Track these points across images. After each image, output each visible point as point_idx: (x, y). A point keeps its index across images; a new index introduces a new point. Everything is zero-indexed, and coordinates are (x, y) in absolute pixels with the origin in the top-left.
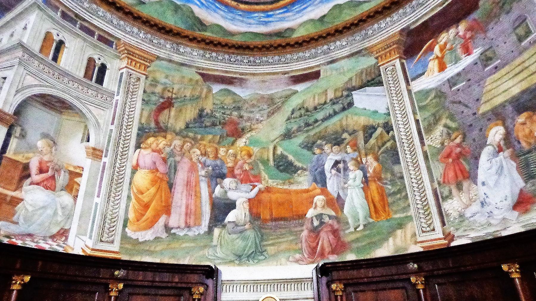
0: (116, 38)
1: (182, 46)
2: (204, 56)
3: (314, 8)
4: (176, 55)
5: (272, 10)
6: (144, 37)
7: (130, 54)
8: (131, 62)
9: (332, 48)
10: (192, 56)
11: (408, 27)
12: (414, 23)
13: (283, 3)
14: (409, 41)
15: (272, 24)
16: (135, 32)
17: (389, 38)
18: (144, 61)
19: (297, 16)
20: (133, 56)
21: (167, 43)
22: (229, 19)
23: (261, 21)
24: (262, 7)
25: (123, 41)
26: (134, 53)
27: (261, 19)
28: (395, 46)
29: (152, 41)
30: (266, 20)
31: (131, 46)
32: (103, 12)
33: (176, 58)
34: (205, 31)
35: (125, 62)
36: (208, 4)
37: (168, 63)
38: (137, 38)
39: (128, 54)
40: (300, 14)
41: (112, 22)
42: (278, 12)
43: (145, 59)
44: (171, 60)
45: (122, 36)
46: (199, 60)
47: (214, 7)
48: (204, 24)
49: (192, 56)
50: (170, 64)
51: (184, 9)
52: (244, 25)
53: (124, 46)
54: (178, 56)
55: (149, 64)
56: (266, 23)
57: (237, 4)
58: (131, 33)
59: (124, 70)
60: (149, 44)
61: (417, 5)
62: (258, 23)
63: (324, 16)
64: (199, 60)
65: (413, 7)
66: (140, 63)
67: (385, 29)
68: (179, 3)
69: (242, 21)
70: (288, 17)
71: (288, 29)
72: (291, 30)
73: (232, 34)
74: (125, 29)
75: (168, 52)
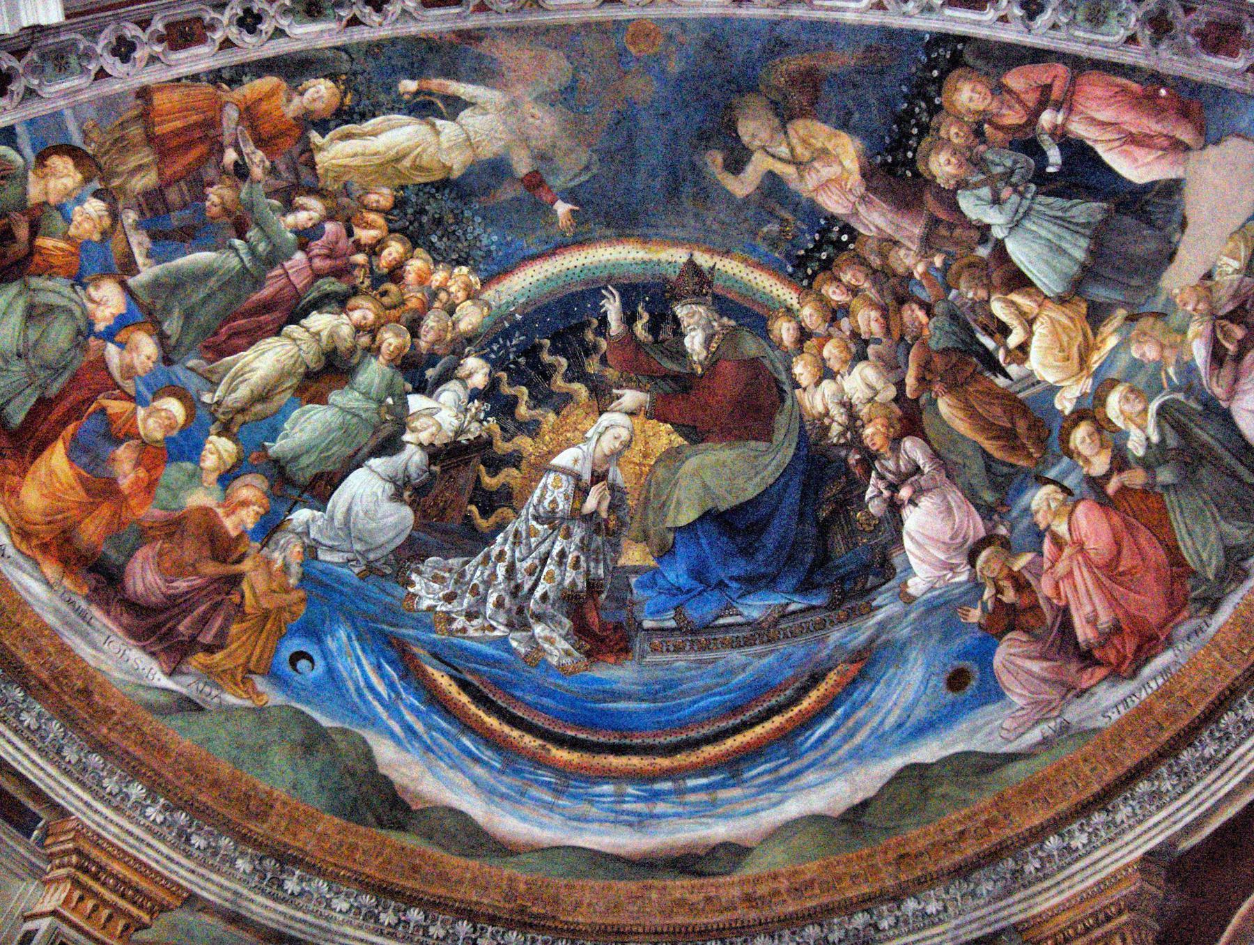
0: (55, 806)
1: (297, 872)
2: (372, 916)
3: (827, 774)
4: (260, 899)
5: (668, 774)
6: (160, 819)
7: (86, 871)
8: (81, 899)
9: (884, 924)
10: (326, 912)
11: (1171, 843)
12: (1189, 830)
13: (713, 753)
14: (1177, 902)
15: (664, 823)
16: (133, 798)
17: (1101, 887)
18: (134, 903)
19: (762, 801)
20: (95, 877)
21: (243, 854)
22: (503, 796)
23: (623, 812)
24: (635, 762)
25: (78, 819)
26: (101, 868)
27: (625, 806)
28: (1125, 918)
29: (188, 840)
30: (641, 807)
31: (97, 841)
32: (40, 716)
33: (262, 908)
34: (401, 827)
35: (56, 895)
36: (434, 741)
37: (222, 925)
38: (130, 818)
39: (79, 867)
40: (775, 796)
41: (59, 751)
42: (691, 783)
43: (137, 896)
44: (238, 914)
45: (80, 805)
46: (348, 930)
47: (456, 752)
48: (404, 802)
49: (326, 912)
50: (232, 929)
51: (342, 745)
52: (558, 819)
53: (73, 839)
54: (269, 903)
55: (146, 918)
56: (640, 822)
57: (543, 747)
58: (118, 802)
59: (44, 924)
60: (173, 846)
61: (1198, 765)
62: (612, 817)
63: (865, 804)
64: (348, 930)
65: (1183, 773)
66: (114, 906)
67: (1089, 853)
68: (325, 722)
69: (550, 807)
70: (730, 801)
71: (725, 845)
72: (735, 852)
73: (503, 849)
74: (100, 784)
75: (234, 886)
